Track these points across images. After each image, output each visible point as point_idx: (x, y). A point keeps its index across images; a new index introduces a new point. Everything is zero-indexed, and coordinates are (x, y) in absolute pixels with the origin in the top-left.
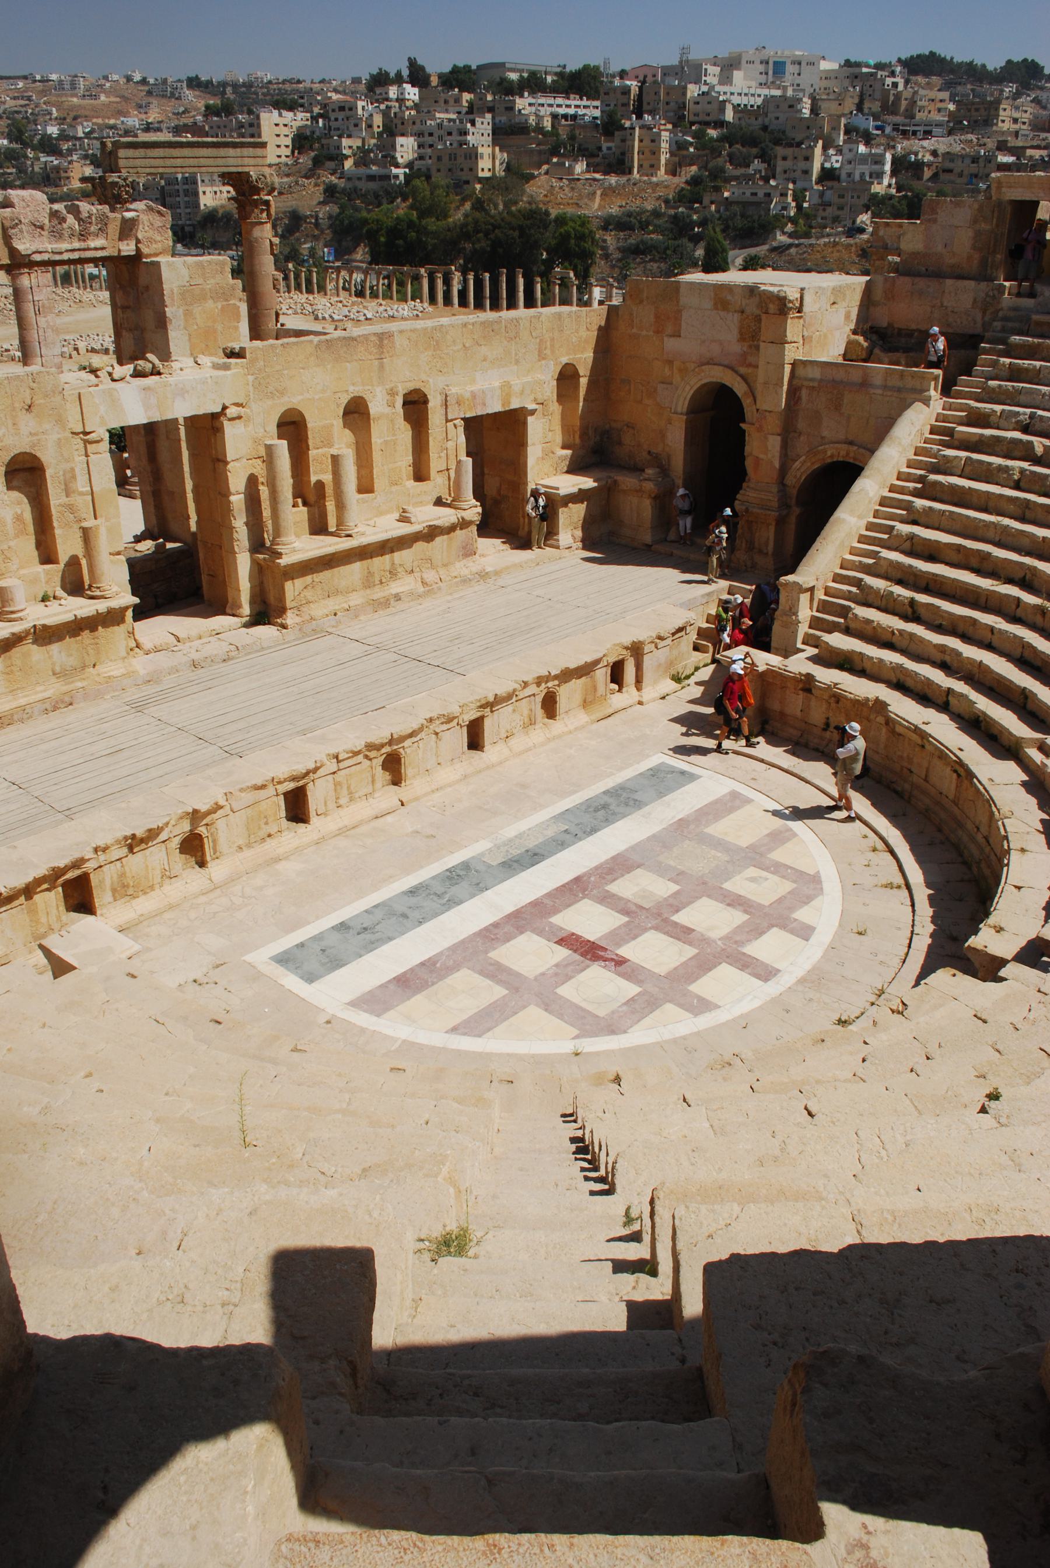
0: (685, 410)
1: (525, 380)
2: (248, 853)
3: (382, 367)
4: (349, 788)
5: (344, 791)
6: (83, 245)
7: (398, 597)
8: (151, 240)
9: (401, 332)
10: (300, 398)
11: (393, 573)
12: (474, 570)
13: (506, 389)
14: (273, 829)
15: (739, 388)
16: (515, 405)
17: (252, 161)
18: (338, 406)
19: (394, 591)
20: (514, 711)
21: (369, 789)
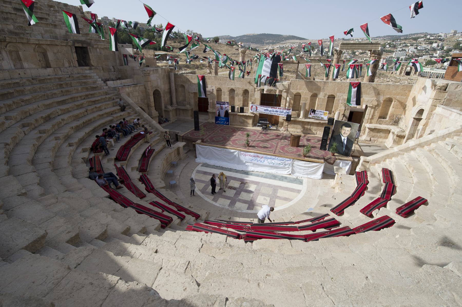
9: (331, 82)
10: (301, 91)
19: (308, 132)
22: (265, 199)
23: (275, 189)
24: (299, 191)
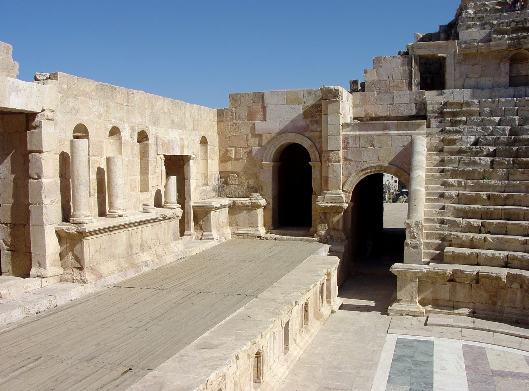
0: (271, 160)
10: (86, 118)
15: (306, 144)
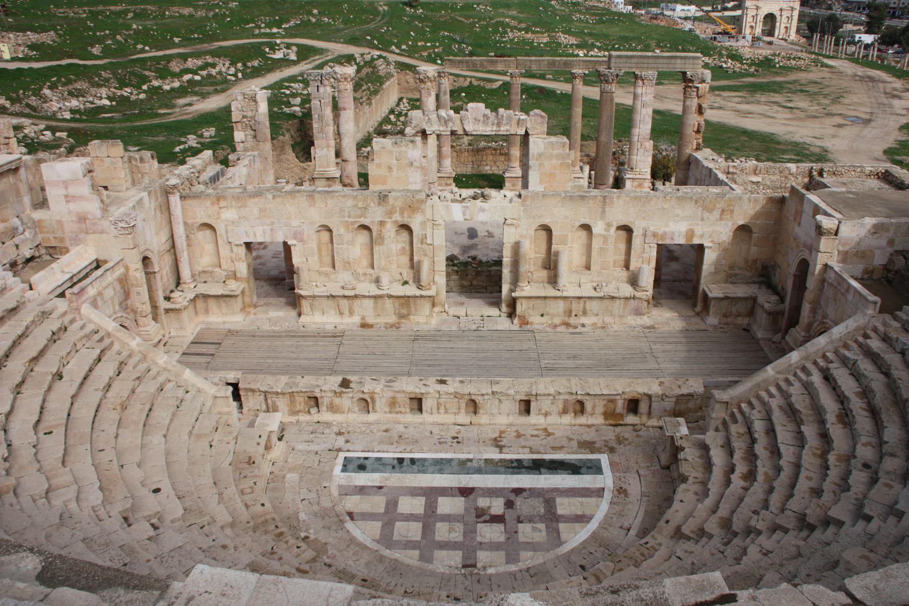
1: (706, 230)
2: (389, 415)
3: (603, 212)
4: (445, 407)
5: (442, 408)
6: (498, 129)
7: (583, 325)
8: (534, 128)
11: (585, 313)
12: (639, 323)
13: (690, 234)
14: (403, 410)
16: (696, 241)
17: (691, 66)
18: (573, 227)
19: (581, 322)
20: (552, 403)
21: (457, 411)
22: (534, 529)
23: (548, 497)
24: (600, 492)
